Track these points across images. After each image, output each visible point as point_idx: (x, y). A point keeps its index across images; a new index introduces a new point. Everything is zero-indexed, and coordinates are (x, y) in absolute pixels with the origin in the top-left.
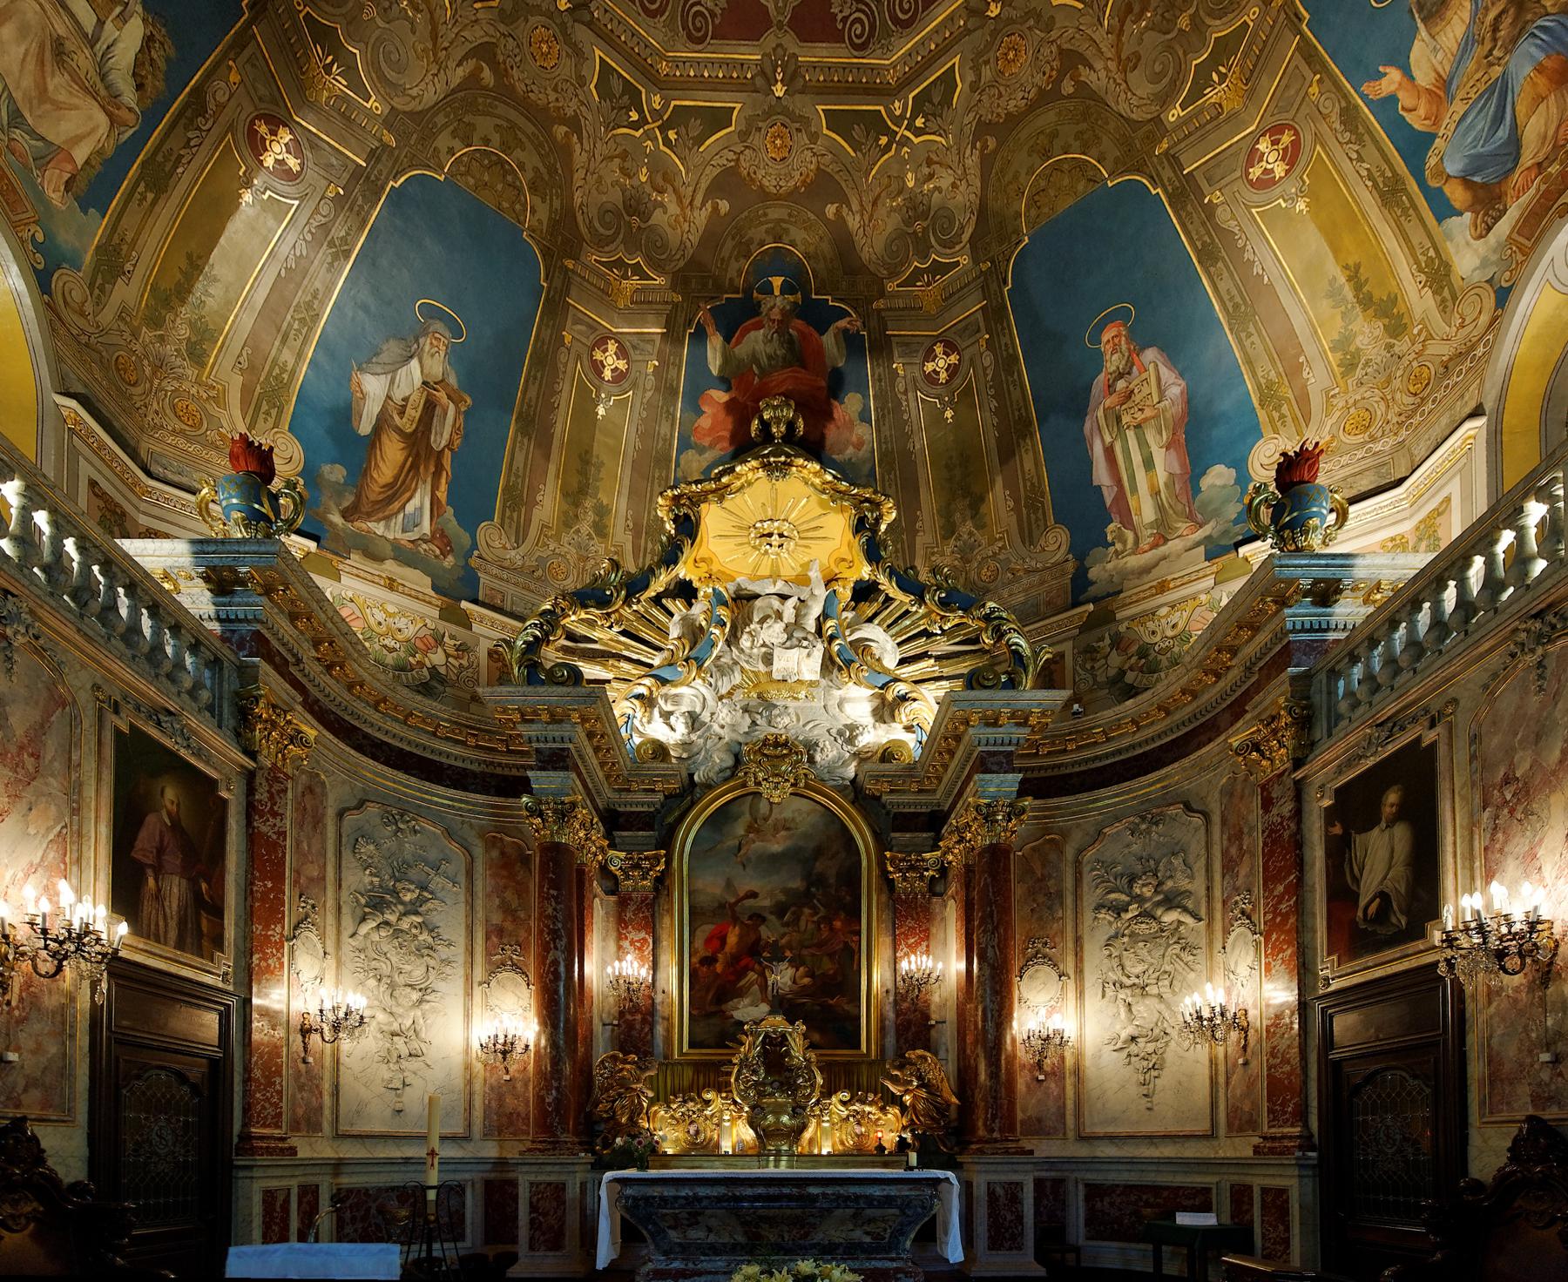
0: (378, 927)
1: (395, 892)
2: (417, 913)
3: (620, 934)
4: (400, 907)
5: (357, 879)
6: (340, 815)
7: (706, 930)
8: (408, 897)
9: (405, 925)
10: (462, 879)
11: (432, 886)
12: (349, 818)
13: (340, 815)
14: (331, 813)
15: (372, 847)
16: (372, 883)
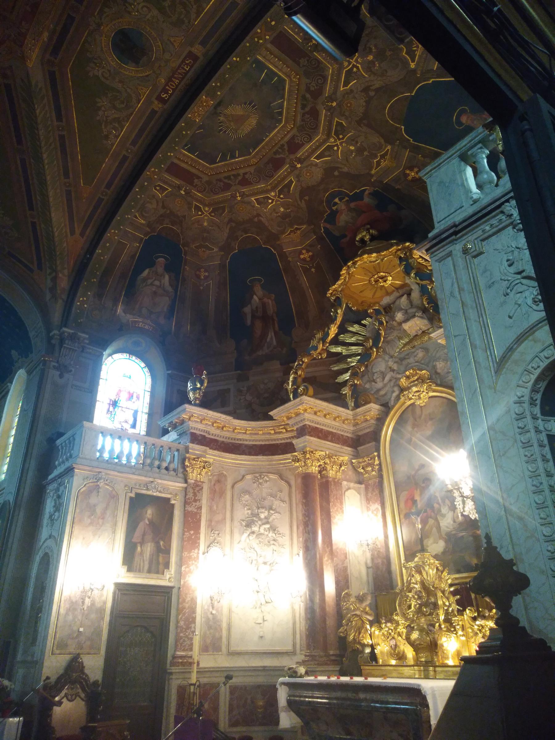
0: (249, 535)
1: (257, 515)
2: (268, 523)
3: (367, 507)
4: (260, 522)
5: (242, 513)
6: (233, 487)
7: (404, 495)
8: (262, 516)
9: (262, 531)
10: (287, 499)
11: (274, 507)
12: (237, 486)
13: (233, 487)
14: (229, 487)
15: (247, 496)
16: (248, 513)
